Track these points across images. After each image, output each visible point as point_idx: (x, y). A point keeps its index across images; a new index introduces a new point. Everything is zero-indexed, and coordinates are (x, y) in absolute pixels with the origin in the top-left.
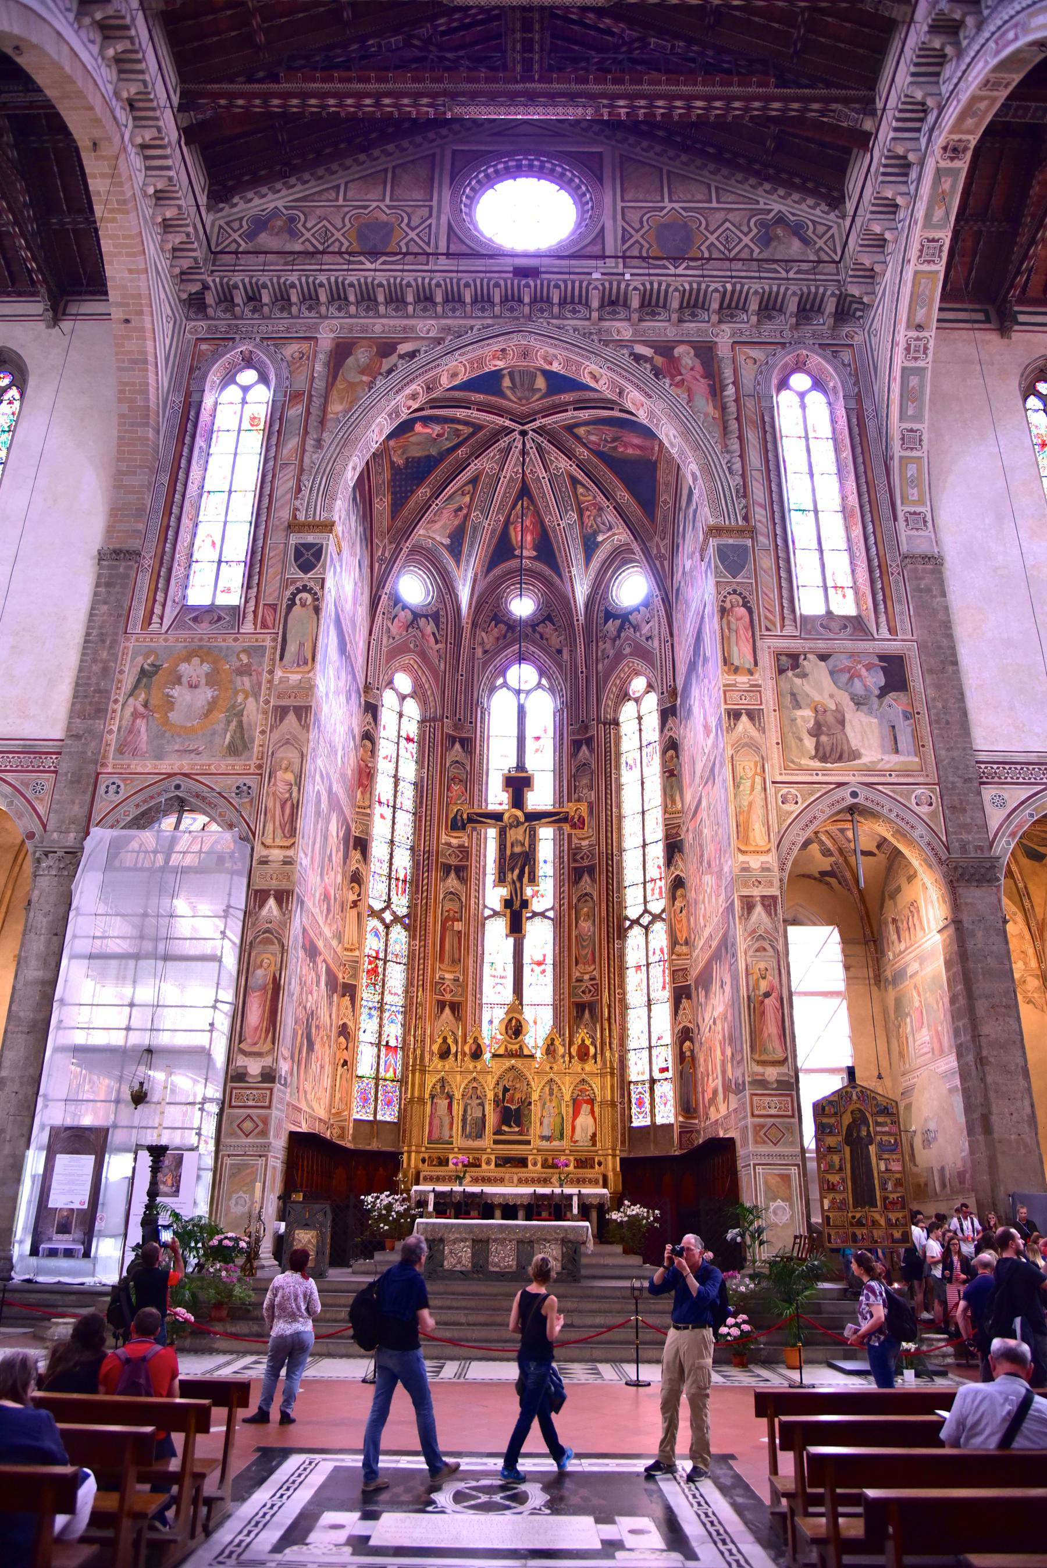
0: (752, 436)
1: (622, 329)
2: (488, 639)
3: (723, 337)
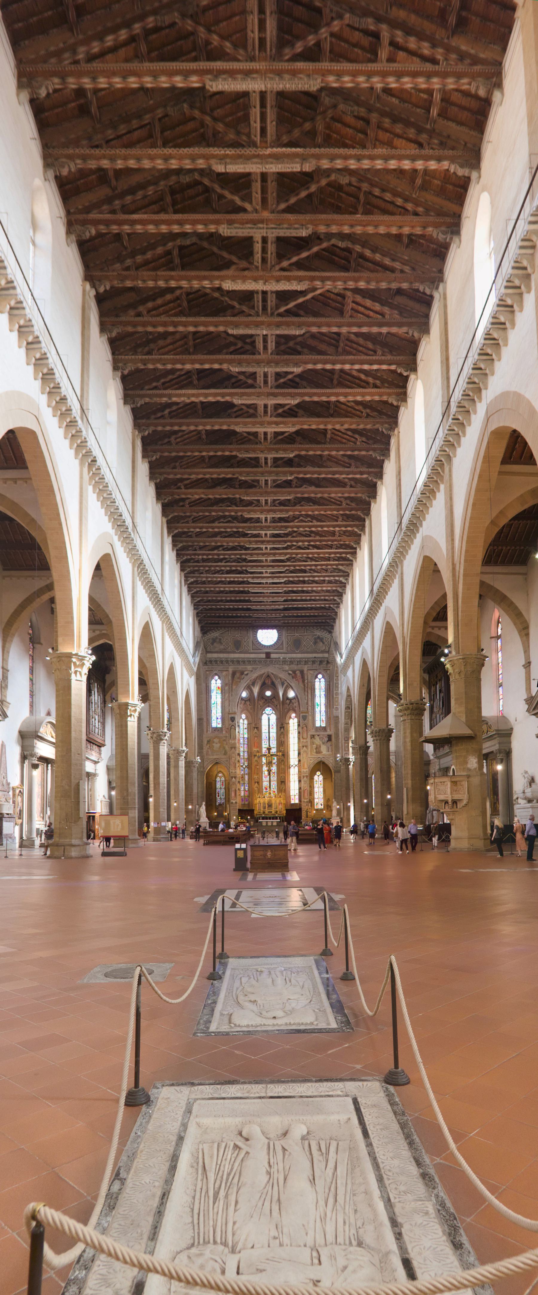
0: (309, 691)
1: (287, 667)
2: (261, 703)
3: (305, 668)
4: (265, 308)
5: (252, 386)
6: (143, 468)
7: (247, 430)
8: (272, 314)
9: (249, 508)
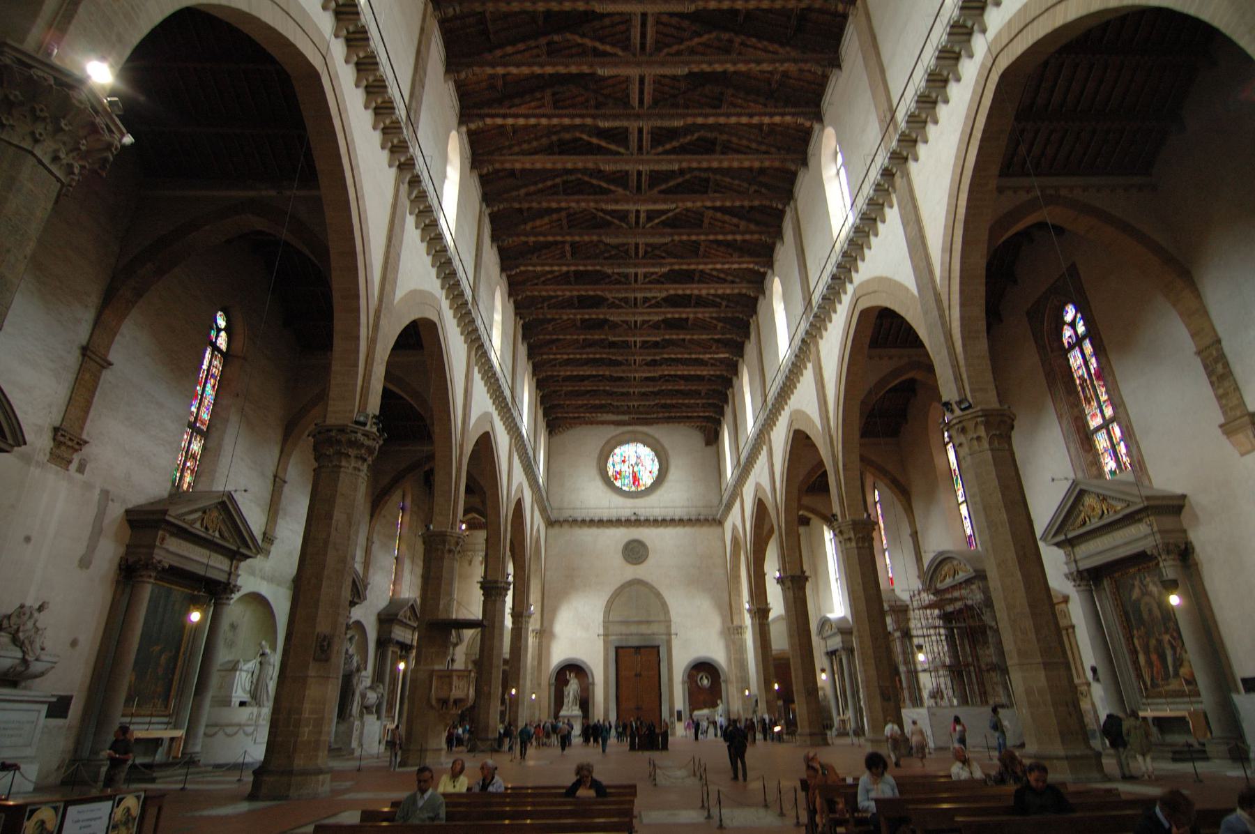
4: (637, 223)
5: (626, 284)
6: (522, 350)
7: (622, 319)
8: (644, 227)
9: (618, 383)
